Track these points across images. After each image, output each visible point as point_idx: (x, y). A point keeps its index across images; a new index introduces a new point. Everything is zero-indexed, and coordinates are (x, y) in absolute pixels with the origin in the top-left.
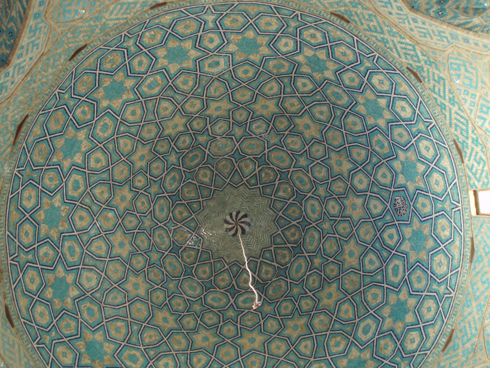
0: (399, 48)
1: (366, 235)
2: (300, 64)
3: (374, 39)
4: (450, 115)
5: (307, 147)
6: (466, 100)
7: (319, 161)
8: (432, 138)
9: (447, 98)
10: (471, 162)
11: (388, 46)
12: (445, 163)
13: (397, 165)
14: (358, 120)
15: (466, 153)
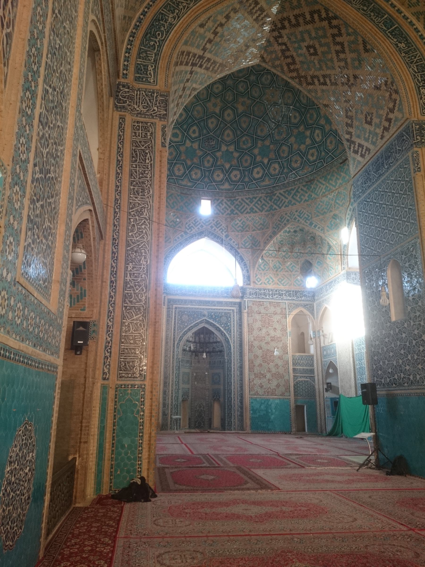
0: (283, 198)
1: (197, 111)
2: (306, 129)
3: (293, 187)
4: (247, 203)
5: (261, 86)
6: (250, 217)
7: (249, 89)
8: (239, 183)
9: (254, 207)
10: (224, 204)
11: (287, 193)
12: (226, 186)
13: (232, 148)
14: (263, 135)
15: (229, 201)
